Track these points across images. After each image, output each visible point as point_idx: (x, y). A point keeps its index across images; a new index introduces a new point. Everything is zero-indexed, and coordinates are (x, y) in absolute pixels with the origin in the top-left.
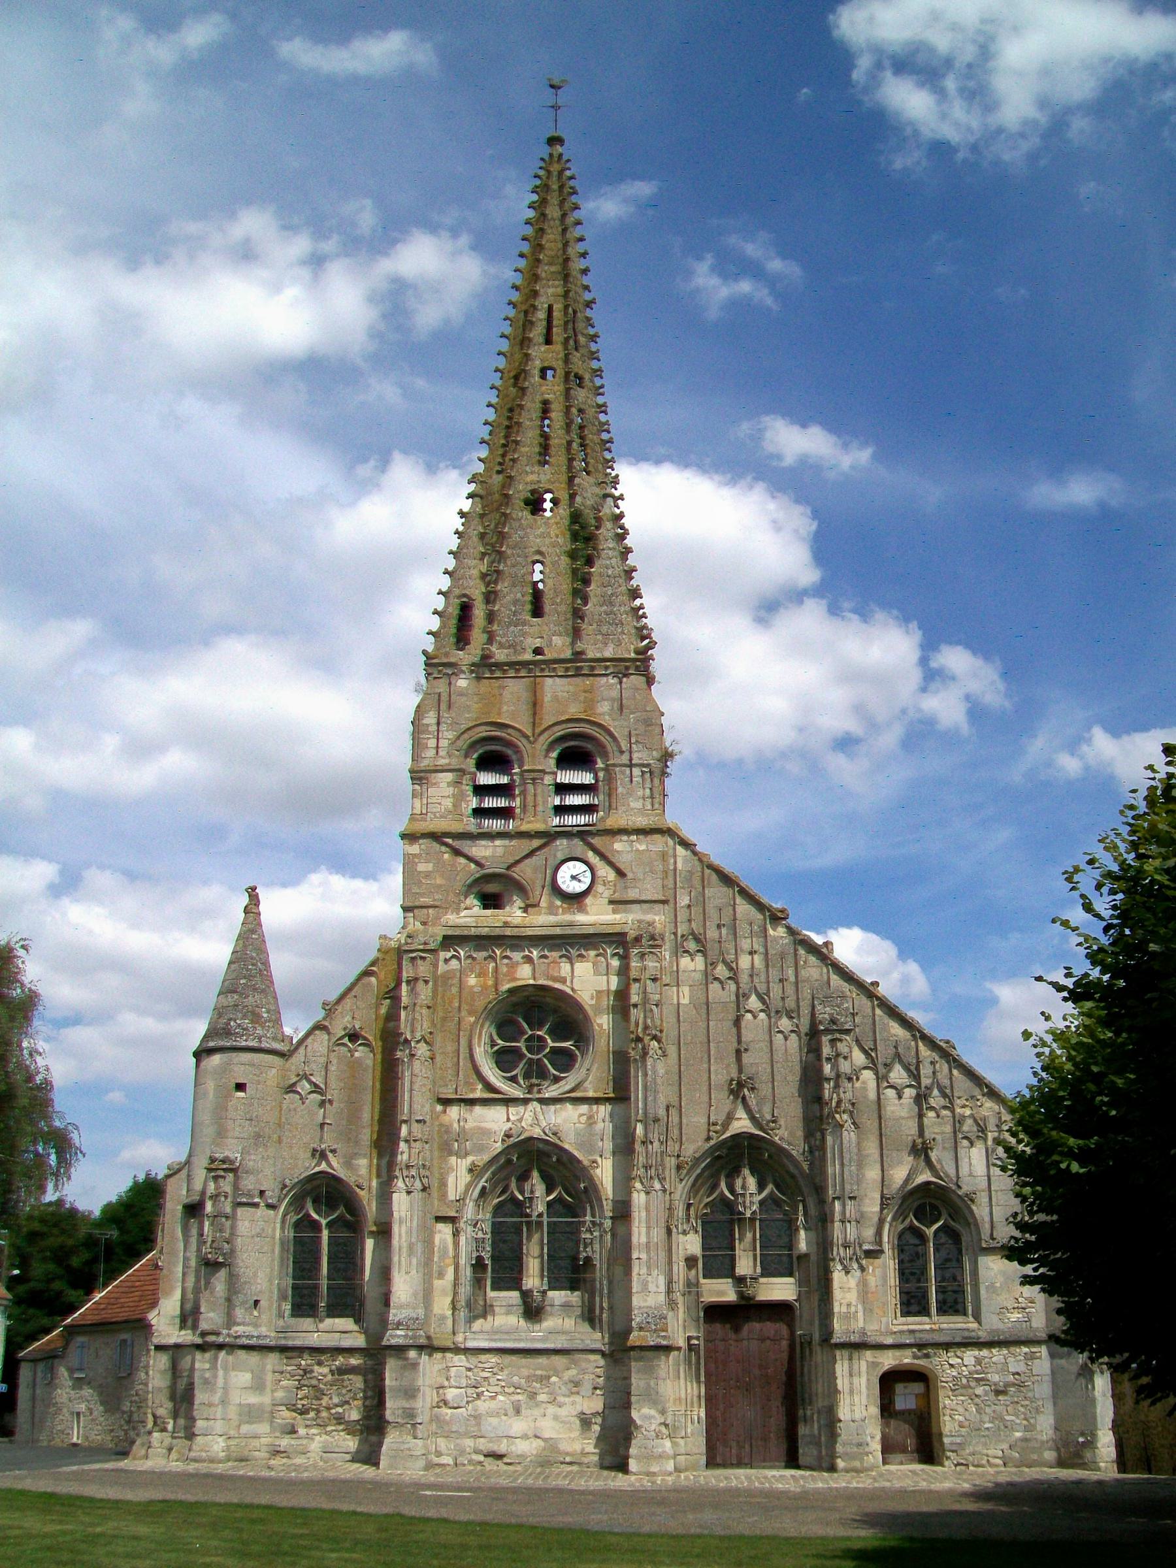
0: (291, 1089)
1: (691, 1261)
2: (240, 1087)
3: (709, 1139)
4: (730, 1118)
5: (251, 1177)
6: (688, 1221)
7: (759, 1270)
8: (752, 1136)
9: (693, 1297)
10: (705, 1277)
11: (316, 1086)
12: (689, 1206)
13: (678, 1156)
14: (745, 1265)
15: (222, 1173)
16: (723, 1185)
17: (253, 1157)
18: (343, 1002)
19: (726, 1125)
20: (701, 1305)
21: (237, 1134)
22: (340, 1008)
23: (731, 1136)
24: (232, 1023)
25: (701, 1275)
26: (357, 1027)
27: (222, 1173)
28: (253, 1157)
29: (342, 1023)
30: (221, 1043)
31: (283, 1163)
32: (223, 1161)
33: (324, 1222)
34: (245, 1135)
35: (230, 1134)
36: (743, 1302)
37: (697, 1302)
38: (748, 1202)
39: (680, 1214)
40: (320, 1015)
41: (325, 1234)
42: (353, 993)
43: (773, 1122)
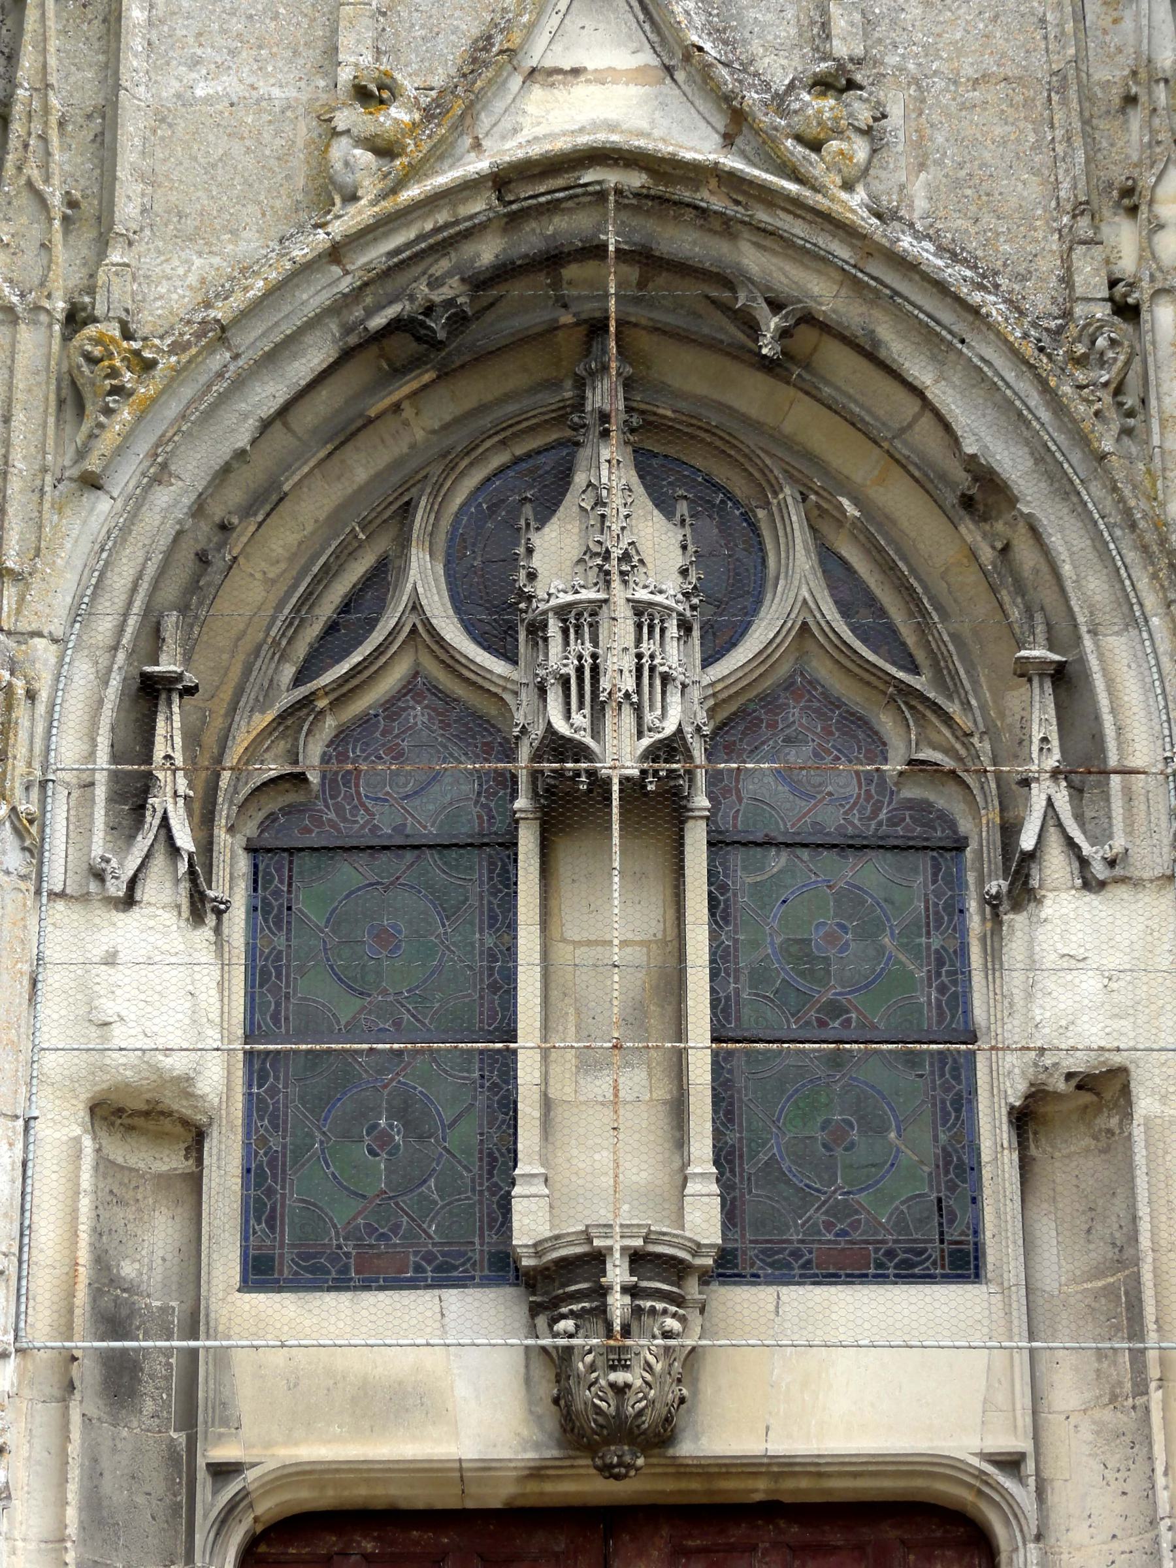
1: (137, 1116)
3: (329, 192)
4: (492, 61)
6: (133, 797)
7: (703, 1222)
8: (667, 182)
9: (147, 1428)
10: (259, 1273)
12: (150, 692)
13: (75, 319)
14: (603, 1160)
16: (425, 578)
19: (456, 109)
20: (210, 1501)
23: (502, 180)
25: (224, 1262)
36: (585, 1485)
37: (182, 1464)
38: (618, 674)
39: (68, 749)
43: (836, 82)
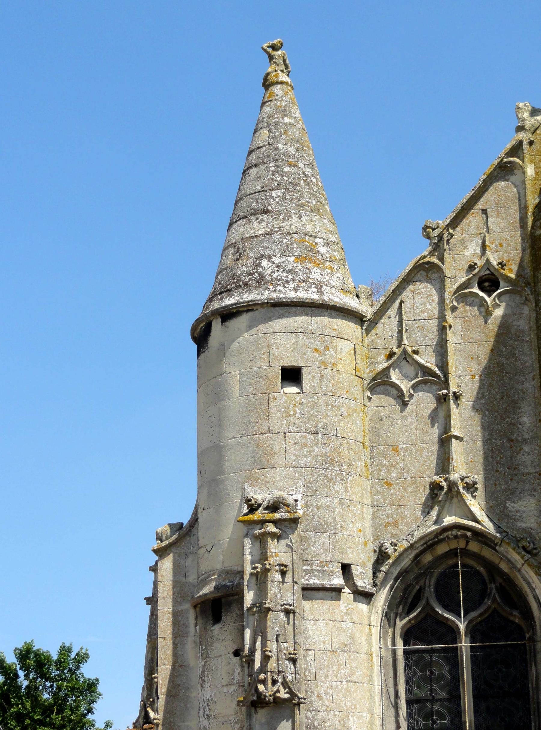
0: (380, 383)
2: (292, 375)
5: (324, 538)
11: (426, 371)
15: (271, 528)
17: (324, 501)
18: (464, 223)
21: (291, 458)
22: (457, 233)
24: (265, 263)
26: (495, 263)
27: (271, 528)
28: (324, 501)
29: (463, 255)
30: (248, 296)
31: (375, 516)
32: (274, 507)
33: (462, 626)
34: (307, 460)
35: (279, 460)
40: (423, 250)
41: (464, 644)
42: (480, 206)
